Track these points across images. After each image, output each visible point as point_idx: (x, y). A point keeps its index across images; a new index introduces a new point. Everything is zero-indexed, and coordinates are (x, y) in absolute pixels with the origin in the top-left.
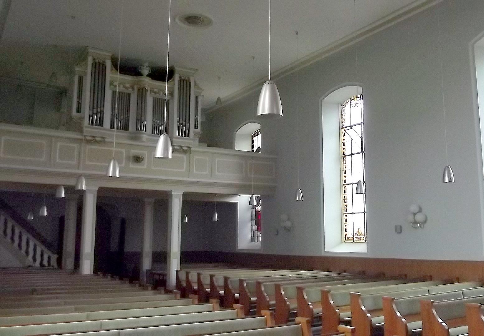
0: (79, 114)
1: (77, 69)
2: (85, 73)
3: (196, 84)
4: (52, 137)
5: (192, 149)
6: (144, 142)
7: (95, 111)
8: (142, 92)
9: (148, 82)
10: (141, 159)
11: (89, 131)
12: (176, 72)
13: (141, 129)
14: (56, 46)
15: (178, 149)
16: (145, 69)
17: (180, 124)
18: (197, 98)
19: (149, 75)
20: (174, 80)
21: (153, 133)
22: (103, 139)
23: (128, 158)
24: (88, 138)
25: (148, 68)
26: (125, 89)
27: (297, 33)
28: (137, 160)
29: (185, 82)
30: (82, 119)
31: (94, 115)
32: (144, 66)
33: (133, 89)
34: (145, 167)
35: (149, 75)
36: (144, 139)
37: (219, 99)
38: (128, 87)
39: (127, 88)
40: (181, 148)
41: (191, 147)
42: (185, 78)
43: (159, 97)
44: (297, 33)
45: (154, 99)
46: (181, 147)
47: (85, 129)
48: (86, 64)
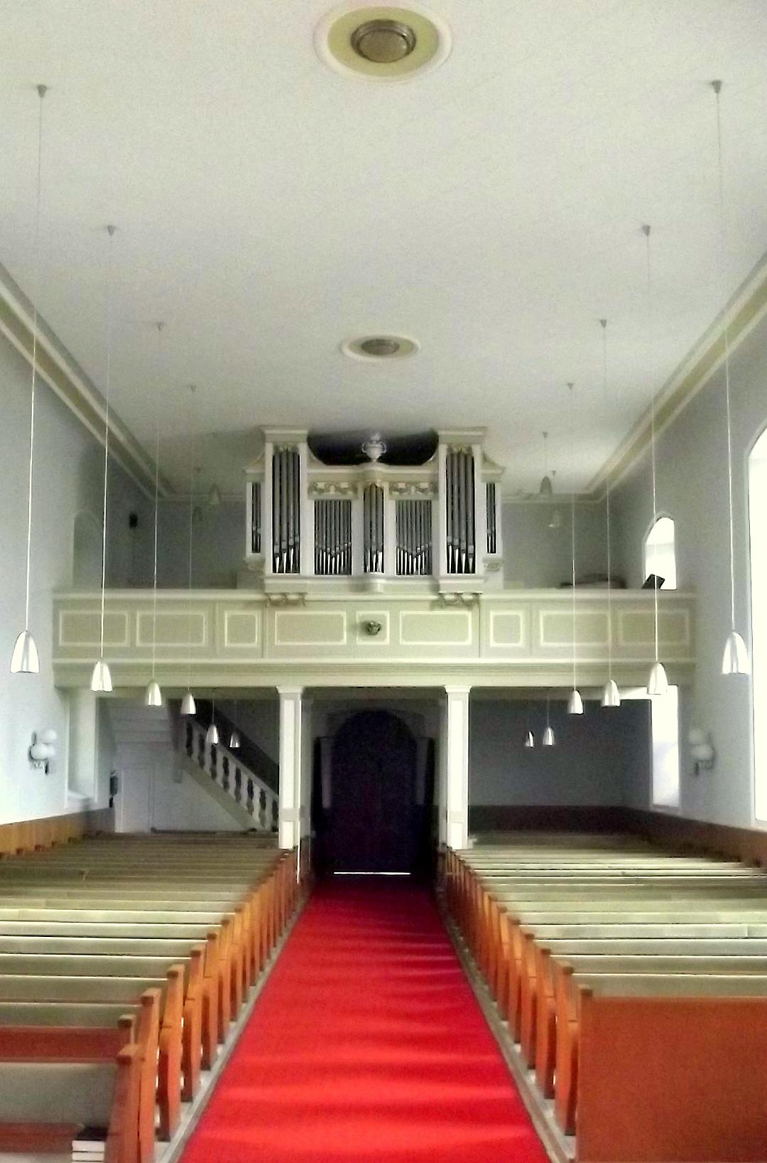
1: (250, 470)
2: (263, 475)
3: (485, 459)
4: (214, 602)
5: (482, 597)
6: (380, 593)
7: (284, 545)
8: (373, 497)
9: (380, 473)
10: (375, 629)
11: (277, 583)
13: (371, 570)
18: (491, 489)
19: (387, 459)
21: (399, 573)
22: (301, 597)
23: (352, 628)
24: (274, 597)
26: (339, 493)
27: (604, 323)
30: (262, 563)
32: (371, 442)
34: (387, 641)
36: (379, 589)
37: (546, 483)
39: (343, 491)
43: (409, 498)
44: (604, 323)
46: (458, 594)
47: (267, 582)
48: (262, 462)
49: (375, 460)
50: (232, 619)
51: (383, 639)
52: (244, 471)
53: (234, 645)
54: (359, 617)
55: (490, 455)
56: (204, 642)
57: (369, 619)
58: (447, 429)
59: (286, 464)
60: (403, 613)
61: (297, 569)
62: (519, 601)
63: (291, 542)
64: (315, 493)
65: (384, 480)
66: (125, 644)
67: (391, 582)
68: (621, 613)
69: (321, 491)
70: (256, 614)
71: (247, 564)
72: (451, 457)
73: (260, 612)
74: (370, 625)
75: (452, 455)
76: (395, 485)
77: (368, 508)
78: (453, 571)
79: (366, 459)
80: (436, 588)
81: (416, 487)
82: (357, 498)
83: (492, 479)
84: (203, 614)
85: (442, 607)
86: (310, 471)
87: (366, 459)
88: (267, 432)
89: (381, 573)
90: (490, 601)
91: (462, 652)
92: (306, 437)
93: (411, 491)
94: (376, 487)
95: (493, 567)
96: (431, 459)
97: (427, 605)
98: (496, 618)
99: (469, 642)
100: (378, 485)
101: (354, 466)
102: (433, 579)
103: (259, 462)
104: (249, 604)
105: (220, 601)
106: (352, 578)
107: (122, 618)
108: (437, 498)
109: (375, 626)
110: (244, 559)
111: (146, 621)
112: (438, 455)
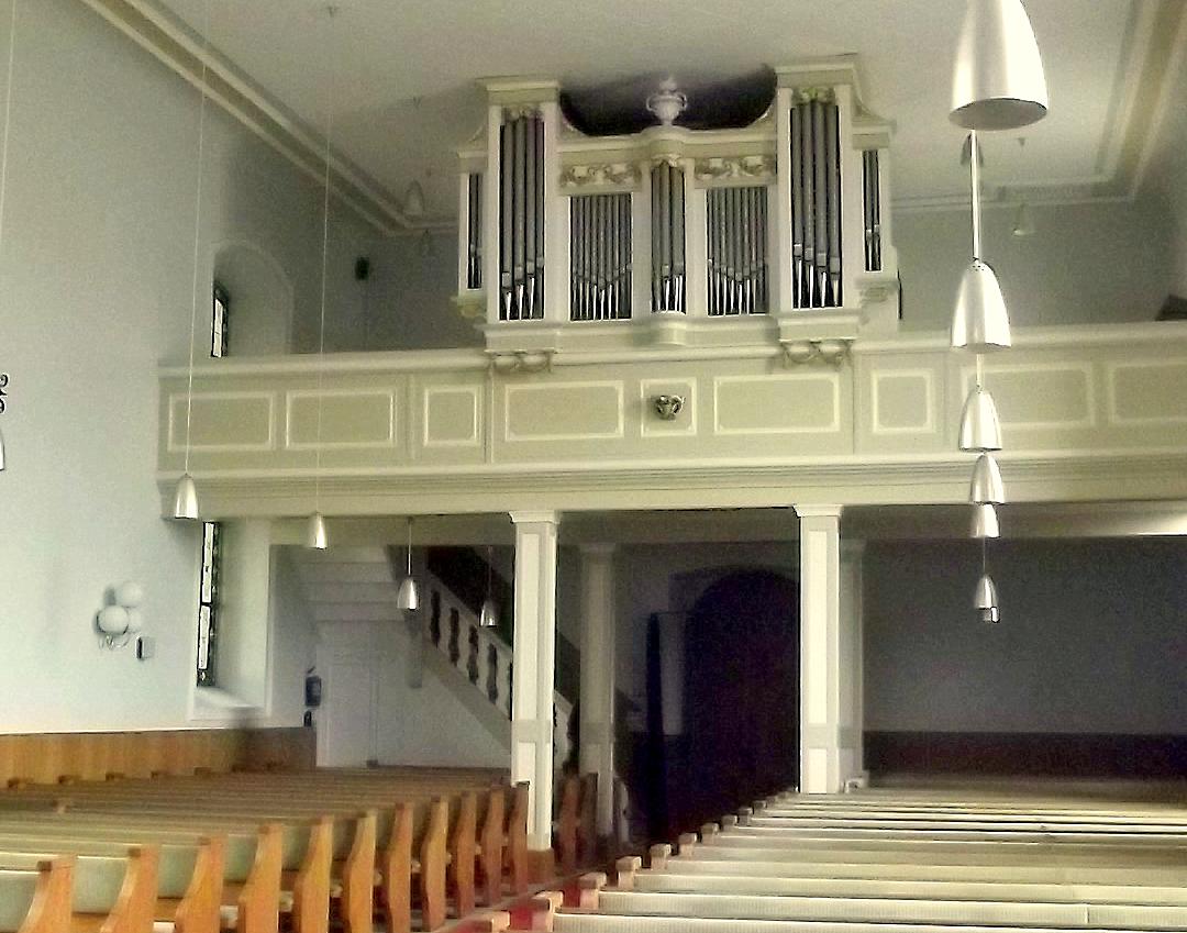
1: (465, 154)
2: (486, 158)
3: (859, 111)
5: (855, 347)
8: (666, 182)
9: (676, 143)
10: (670, 408)
11: (504, 336)
12: (780, 82)
14: (417, 101)
16: (668, 101)
18: (870, 161)
19: (686, 120)
20: (773, 118)
23: (633, 408)
24: (501, 361)
25: (676, 97)
29: (819, 110)
30: (482, 306)
33: (637, 174)
34: (693, 429)
38: (621, 174)
39: (616, 179)
40: (813, 350)
42: (813, 96)
45: (712, 196)
48: (484, 136)
50: (434, 399)
53: (441, 443)
54: (645, 390)
55: (876, 106)
56: (391, 440)
57: (657, 393)
58: (794, 62)
59: (523, 134)
60: (719, 381)
61: (539, 311)
62: (921, 352)
63: (531, 267)
64: (571, 184)
66: (269, 444)
67: (697, 328)
68: (1112, 368)
69: (581, 180)
70: (474, 390)
71: (461, 307)
72: (799, 109)
73: (481, 386)
74: (659, 401)
78: (806, 304)
80: (774, 335)
81: (741, 165)
82: (639, 188)
83: (870, 144)
84: (390, 393)
85: (784, 367)
86: (561, 147)
88: (492, 87)
90: (867, 354)
91: (914, 443)
92: (554, 96)
93: (732, 172)
94: (671, 168)
95: (874, 294)
98: (882, 383)
100: (673, 164)
104: (463, 374)
105: (417, 372)
106: (633, 323)
107: (264, 403)
110: (453, 299)
111: (303, 411)
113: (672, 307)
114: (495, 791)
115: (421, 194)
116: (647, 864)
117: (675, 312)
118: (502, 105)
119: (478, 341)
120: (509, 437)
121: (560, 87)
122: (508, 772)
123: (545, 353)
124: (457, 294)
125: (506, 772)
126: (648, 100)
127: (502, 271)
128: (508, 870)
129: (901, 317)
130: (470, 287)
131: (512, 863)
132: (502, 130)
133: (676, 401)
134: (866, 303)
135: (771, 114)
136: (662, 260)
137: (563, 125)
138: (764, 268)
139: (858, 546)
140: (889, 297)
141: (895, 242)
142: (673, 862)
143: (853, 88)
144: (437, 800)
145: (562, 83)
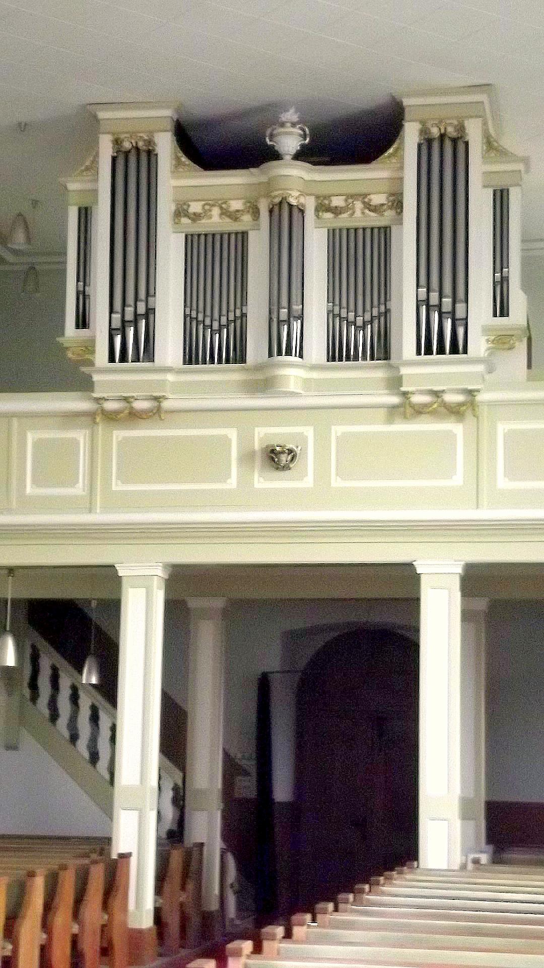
0: (83, 332)
2: (95, 192)
5: (480, 397)
10: (284, 458)
12: (407, 116)
15: (426, 405)
17: (431, 308)
18: (501, 199)
20: (400, 148)
22: (156, 404)
23: (247, 457)
24: (110, 406)
25: (297, 130)
26: (228, 220)
28: (273, 459)
30: (90, 347)
31: (127, 329)
33: (256, 213)
34: (308, 482)
35: (302, 155)
38: (238, 211)
39: (234, 216)
40: (435, 399)
41: (478, 391)
42: (443, 131)
45: (333, 234)
46: (436, 394)
48: (93, 168)
49: (288, 158)
51: (303, 476)
52: (66, 187)
54: (261, 440)
55: (508, 142)
57: (274, 442)
60: (338, 430)
61: (149, 354)
63: (141, 309)
64: (185, 220)
65: (303, 194)
67: (315, 375)
69: (196, 217)
70: (81, 436)
72: (426, 144)
74: (273, 451)
75: (429, 142)
76: (326, 202)
77: (276, 241)
79: (274, 155)
80: (395, 383)
81: (364, 203)
82: (257, 228)
83: (500, 183)
85: (405, 417)
87: (274, 155)
88: (101, 115)
89: (298, 359)
90: (492, 404)
92: (170, 125)
93: (354, 213)
94: (291, 206)
95: (502, 341)
96: (391, 150)
97: (382, 412)
99: (458, 480)
100: (293, 202)
101: (252, 170)
102: (390, 366)
103: (87, 169)
104: (70, 418)
106: (246, 370)
108: (400, 222)
109: (283, 452)
112: (402, 143)
113: (289, 353)
114: (95, 862)
115: (27, 227)
116: (258, 949)
117: (289, 358)
118: (113, 134)
119: (85, 385)
120: (117, 486)
121: (175, 117)
122: (108, 841)
123: (156, 399)
124: (63, 334)
125: (107, 841)
126: (268, 132)
127: (111, 311)
128: (106, 951)
129: (529, 366)
130: (77, 327)
131: (110, 942)
132: (114, 159)
133: (290, 451)
134: (492, 352)
135: (397, 150)
136: (279, 302)
137: (178, 159)
138: (387, 312)
139: (481, 604)
140: (517, 344)
141: (526, 286)
142: (286, 945)
143: (485, 124)
144: (31, 875)
145: (178, 110)
